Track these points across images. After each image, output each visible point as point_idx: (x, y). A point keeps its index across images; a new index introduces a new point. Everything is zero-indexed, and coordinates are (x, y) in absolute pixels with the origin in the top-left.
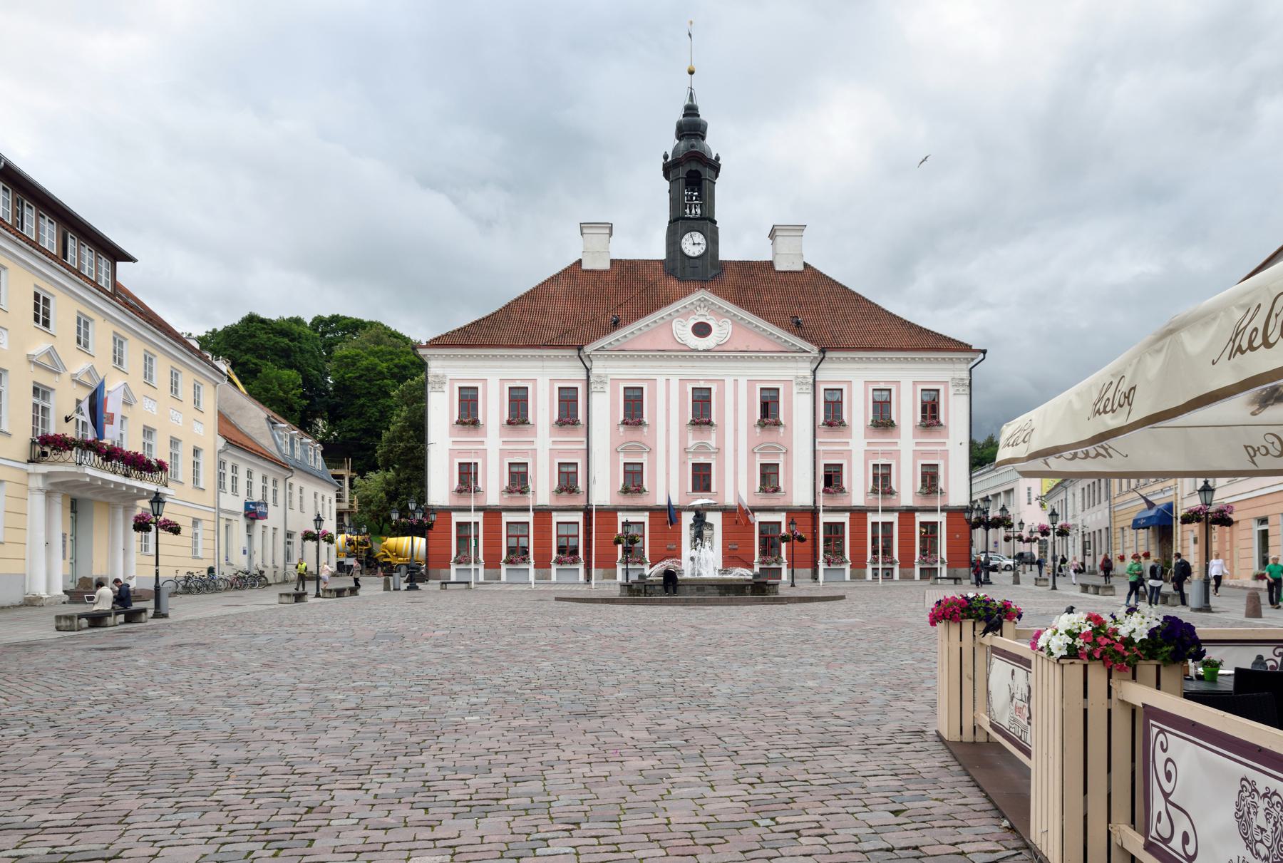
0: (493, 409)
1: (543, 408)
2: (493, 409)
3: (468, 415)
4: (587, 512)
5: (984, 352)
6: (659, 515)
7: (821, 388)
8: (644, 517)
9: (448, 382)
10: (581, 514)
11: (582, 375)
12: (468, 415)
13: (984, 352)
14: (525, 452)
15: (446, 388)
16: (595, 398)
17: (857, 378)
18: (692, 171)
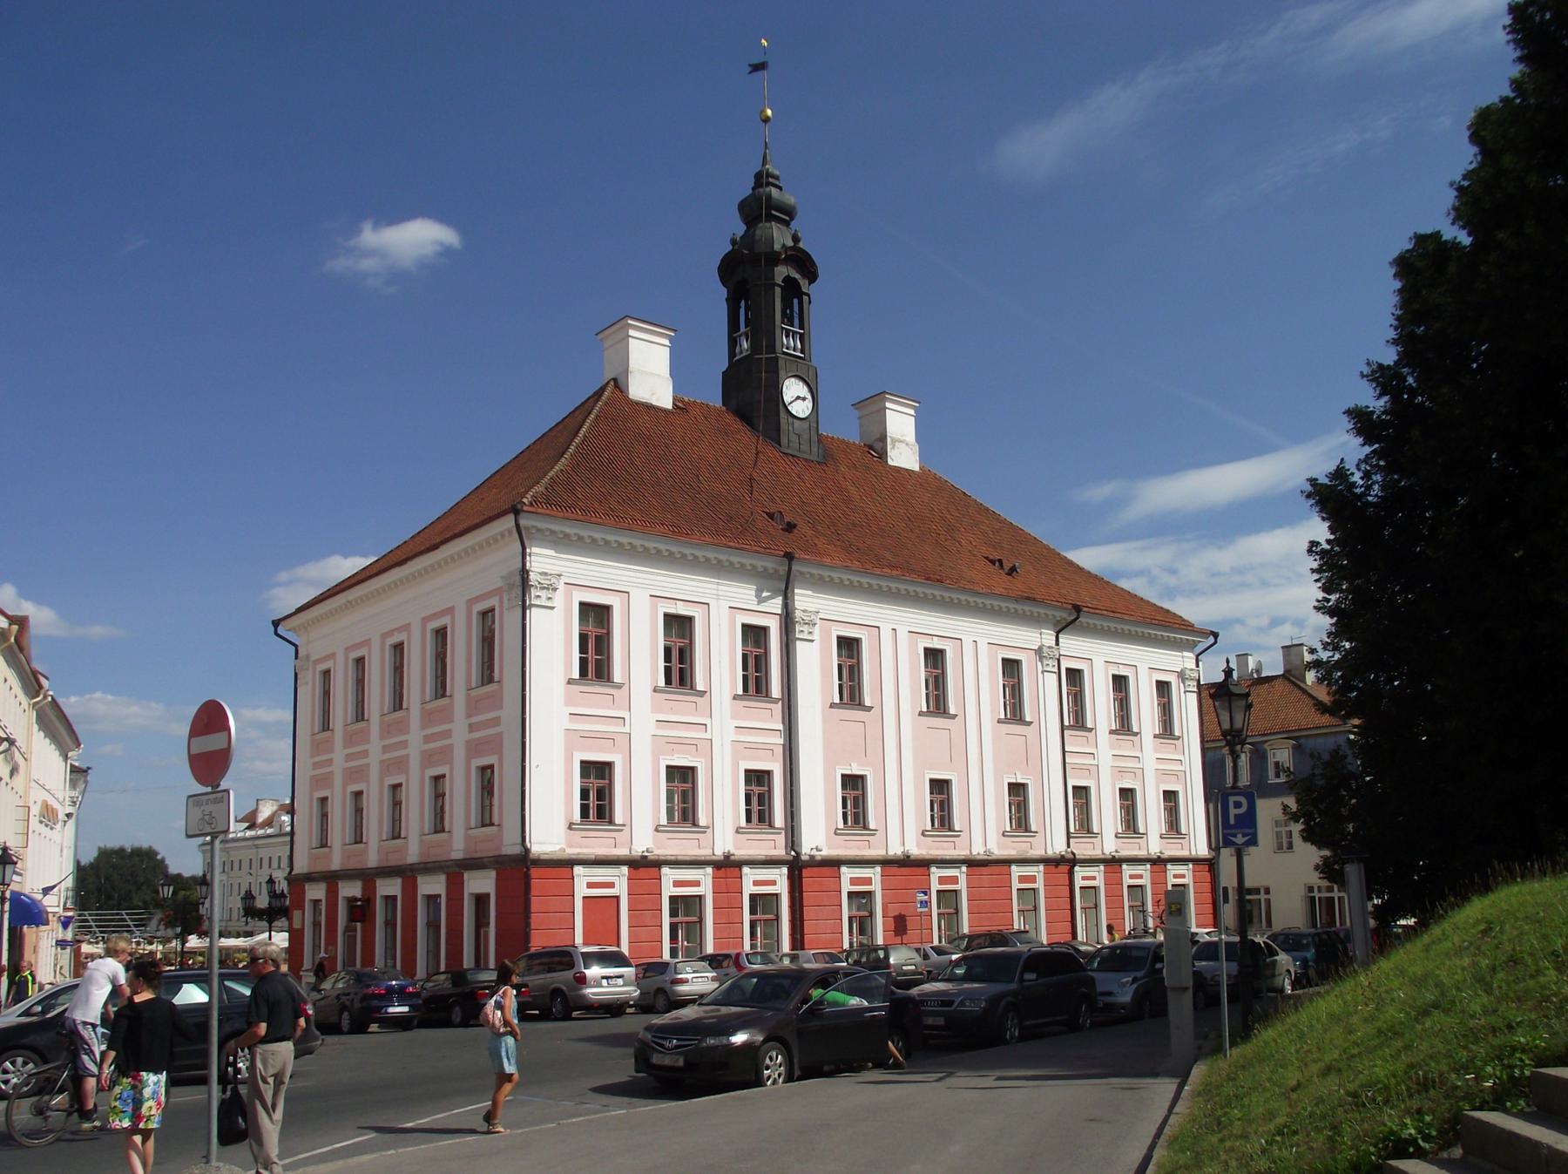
0: (639, 650)
1: (719, 659)
2: (639, 650)
3: (595, 660)
4: (797, 868)
5: (1216, 635)
6: (894, 870)
7: (1065, 664)
8: (875, 873)
9: (561, 587)
10: (785, 870)
11: (776, 605)
12: (595, 660)
13: (1216, 635)
14: (694, 745)
15: (559, 599)
16: (802, 651)
17: (1099, 657)
18: (762, 284)
